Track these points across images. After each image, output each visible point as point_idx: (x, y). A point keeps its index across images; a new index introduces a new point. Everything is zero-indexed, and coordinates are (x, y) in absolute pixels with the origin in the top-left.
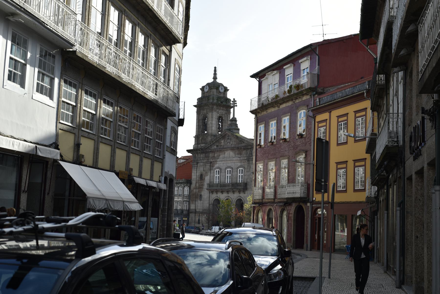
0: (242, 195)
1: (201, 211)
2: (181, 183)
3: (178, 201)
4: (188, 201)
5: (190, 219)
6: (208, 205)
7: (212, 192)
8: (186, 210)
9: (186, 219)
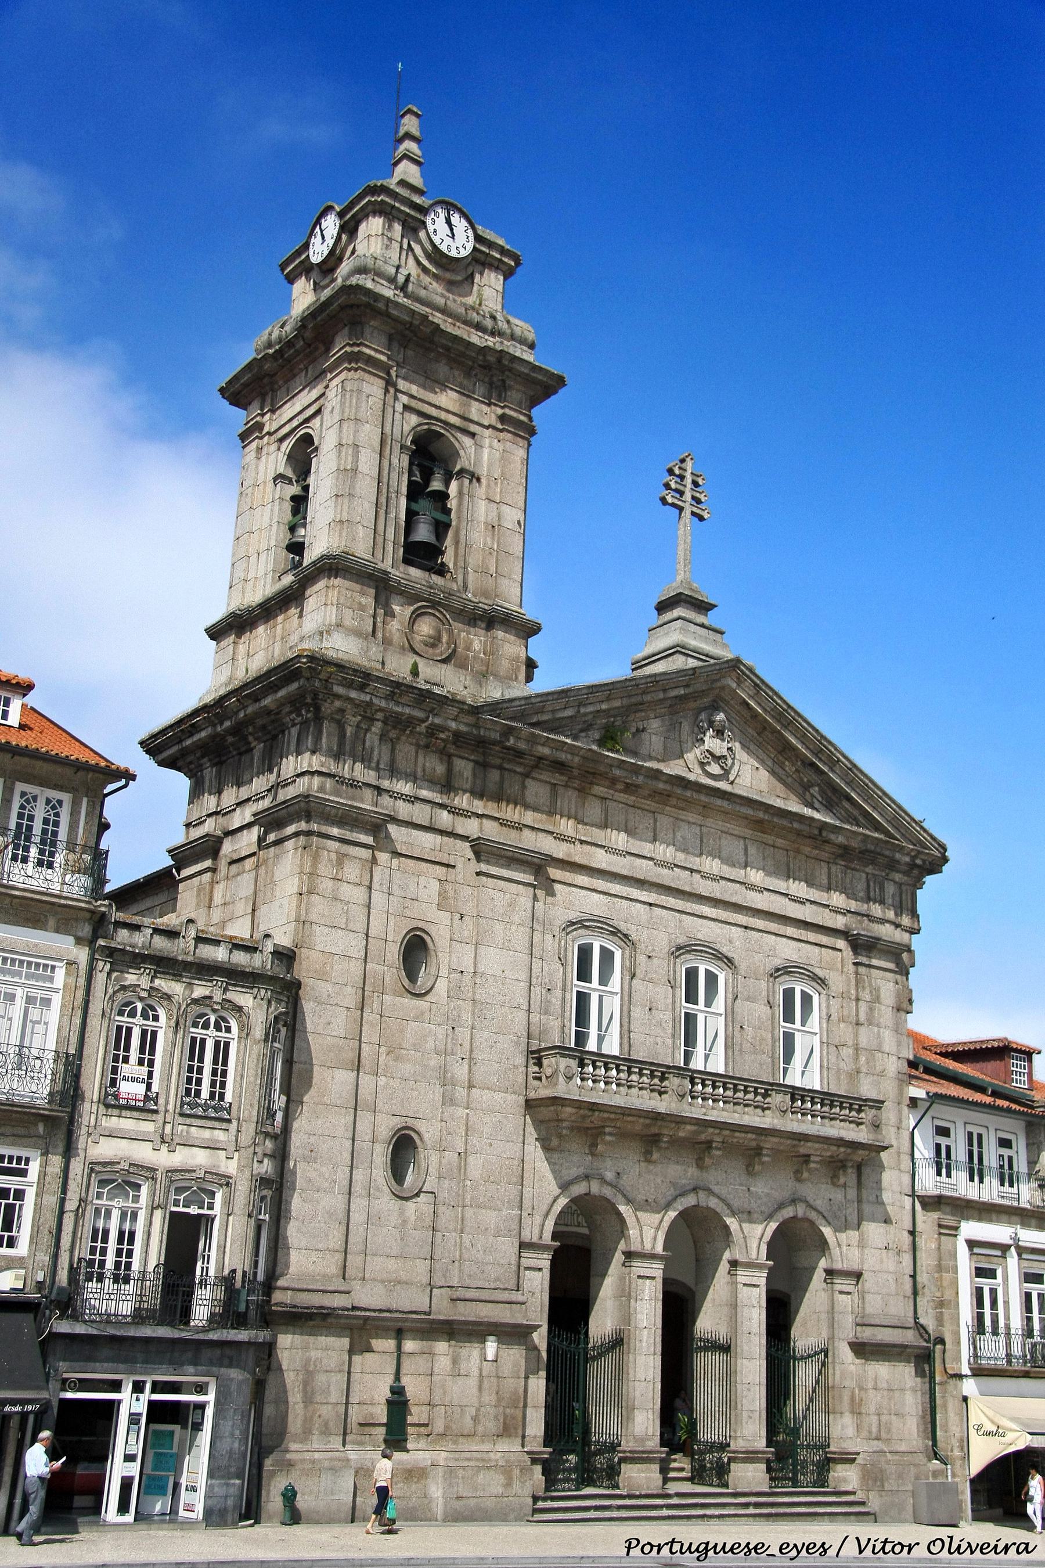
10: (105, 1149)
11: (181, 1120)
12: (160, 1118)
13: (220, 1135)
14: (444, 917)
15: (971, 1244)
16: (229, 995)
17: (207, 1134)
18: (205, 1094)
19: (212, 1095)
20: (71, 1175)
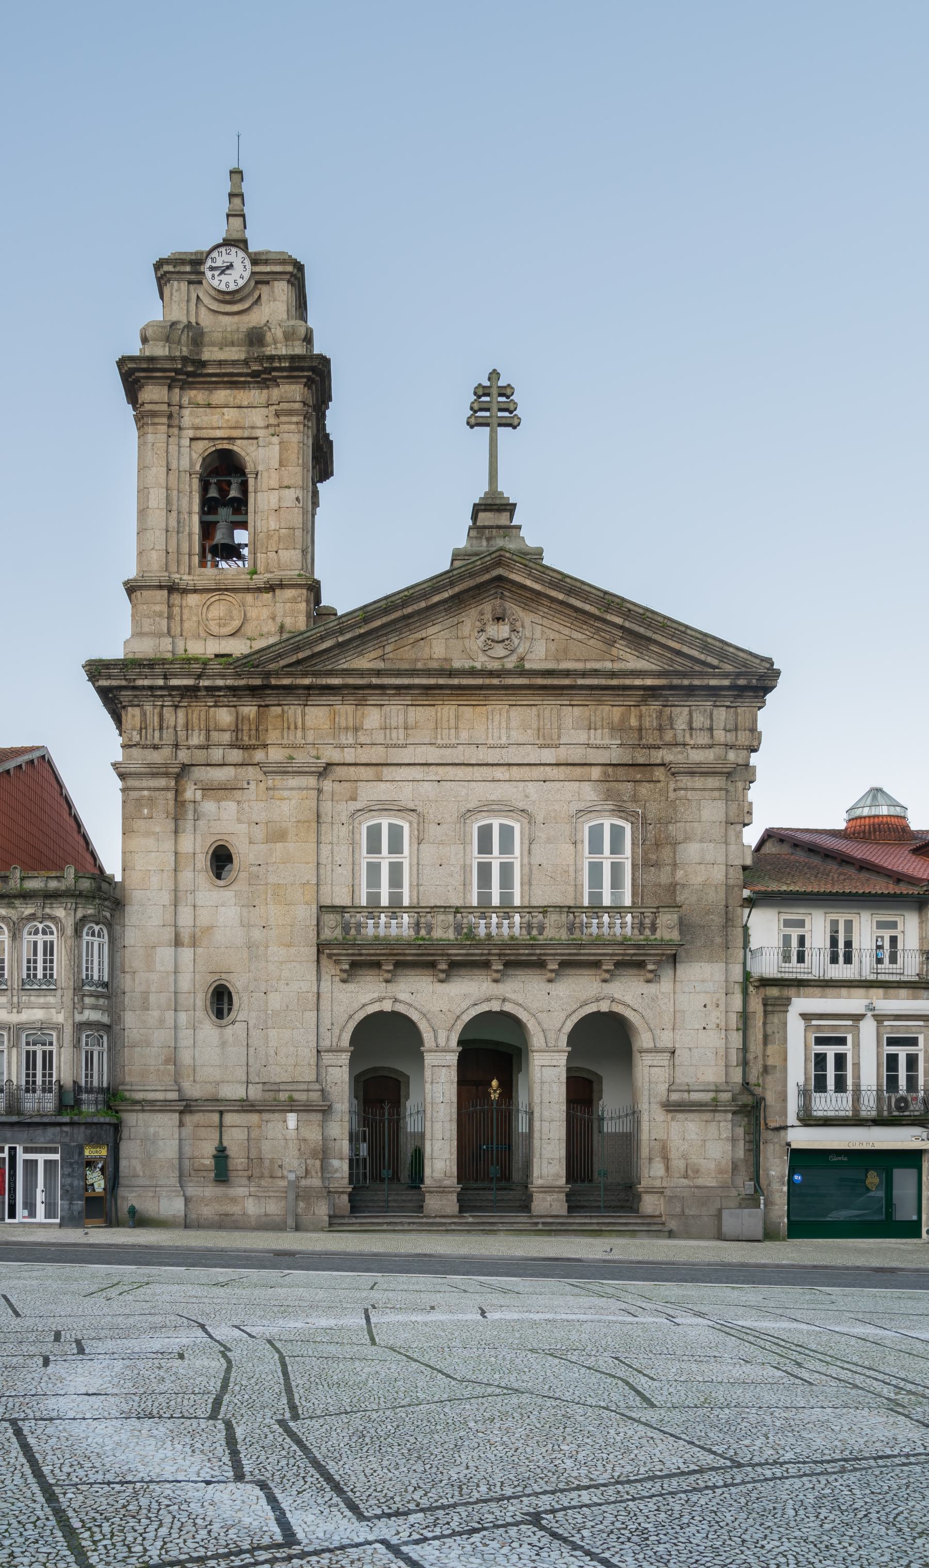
0: (627, 995)
1: (234, 1091)
3: (20, 1028)
4: (108, 1028)
5: (130, 1150)
6: (309, 1054)
9: (104, 1152)
11: (23, 993)
12: (9, 992)
13: (51, 999)
14: (243, 828)
15: (806, 1017)
16: (47, 910)
17: (42, 1000)
18: (40, 975)
19: (45, 976)
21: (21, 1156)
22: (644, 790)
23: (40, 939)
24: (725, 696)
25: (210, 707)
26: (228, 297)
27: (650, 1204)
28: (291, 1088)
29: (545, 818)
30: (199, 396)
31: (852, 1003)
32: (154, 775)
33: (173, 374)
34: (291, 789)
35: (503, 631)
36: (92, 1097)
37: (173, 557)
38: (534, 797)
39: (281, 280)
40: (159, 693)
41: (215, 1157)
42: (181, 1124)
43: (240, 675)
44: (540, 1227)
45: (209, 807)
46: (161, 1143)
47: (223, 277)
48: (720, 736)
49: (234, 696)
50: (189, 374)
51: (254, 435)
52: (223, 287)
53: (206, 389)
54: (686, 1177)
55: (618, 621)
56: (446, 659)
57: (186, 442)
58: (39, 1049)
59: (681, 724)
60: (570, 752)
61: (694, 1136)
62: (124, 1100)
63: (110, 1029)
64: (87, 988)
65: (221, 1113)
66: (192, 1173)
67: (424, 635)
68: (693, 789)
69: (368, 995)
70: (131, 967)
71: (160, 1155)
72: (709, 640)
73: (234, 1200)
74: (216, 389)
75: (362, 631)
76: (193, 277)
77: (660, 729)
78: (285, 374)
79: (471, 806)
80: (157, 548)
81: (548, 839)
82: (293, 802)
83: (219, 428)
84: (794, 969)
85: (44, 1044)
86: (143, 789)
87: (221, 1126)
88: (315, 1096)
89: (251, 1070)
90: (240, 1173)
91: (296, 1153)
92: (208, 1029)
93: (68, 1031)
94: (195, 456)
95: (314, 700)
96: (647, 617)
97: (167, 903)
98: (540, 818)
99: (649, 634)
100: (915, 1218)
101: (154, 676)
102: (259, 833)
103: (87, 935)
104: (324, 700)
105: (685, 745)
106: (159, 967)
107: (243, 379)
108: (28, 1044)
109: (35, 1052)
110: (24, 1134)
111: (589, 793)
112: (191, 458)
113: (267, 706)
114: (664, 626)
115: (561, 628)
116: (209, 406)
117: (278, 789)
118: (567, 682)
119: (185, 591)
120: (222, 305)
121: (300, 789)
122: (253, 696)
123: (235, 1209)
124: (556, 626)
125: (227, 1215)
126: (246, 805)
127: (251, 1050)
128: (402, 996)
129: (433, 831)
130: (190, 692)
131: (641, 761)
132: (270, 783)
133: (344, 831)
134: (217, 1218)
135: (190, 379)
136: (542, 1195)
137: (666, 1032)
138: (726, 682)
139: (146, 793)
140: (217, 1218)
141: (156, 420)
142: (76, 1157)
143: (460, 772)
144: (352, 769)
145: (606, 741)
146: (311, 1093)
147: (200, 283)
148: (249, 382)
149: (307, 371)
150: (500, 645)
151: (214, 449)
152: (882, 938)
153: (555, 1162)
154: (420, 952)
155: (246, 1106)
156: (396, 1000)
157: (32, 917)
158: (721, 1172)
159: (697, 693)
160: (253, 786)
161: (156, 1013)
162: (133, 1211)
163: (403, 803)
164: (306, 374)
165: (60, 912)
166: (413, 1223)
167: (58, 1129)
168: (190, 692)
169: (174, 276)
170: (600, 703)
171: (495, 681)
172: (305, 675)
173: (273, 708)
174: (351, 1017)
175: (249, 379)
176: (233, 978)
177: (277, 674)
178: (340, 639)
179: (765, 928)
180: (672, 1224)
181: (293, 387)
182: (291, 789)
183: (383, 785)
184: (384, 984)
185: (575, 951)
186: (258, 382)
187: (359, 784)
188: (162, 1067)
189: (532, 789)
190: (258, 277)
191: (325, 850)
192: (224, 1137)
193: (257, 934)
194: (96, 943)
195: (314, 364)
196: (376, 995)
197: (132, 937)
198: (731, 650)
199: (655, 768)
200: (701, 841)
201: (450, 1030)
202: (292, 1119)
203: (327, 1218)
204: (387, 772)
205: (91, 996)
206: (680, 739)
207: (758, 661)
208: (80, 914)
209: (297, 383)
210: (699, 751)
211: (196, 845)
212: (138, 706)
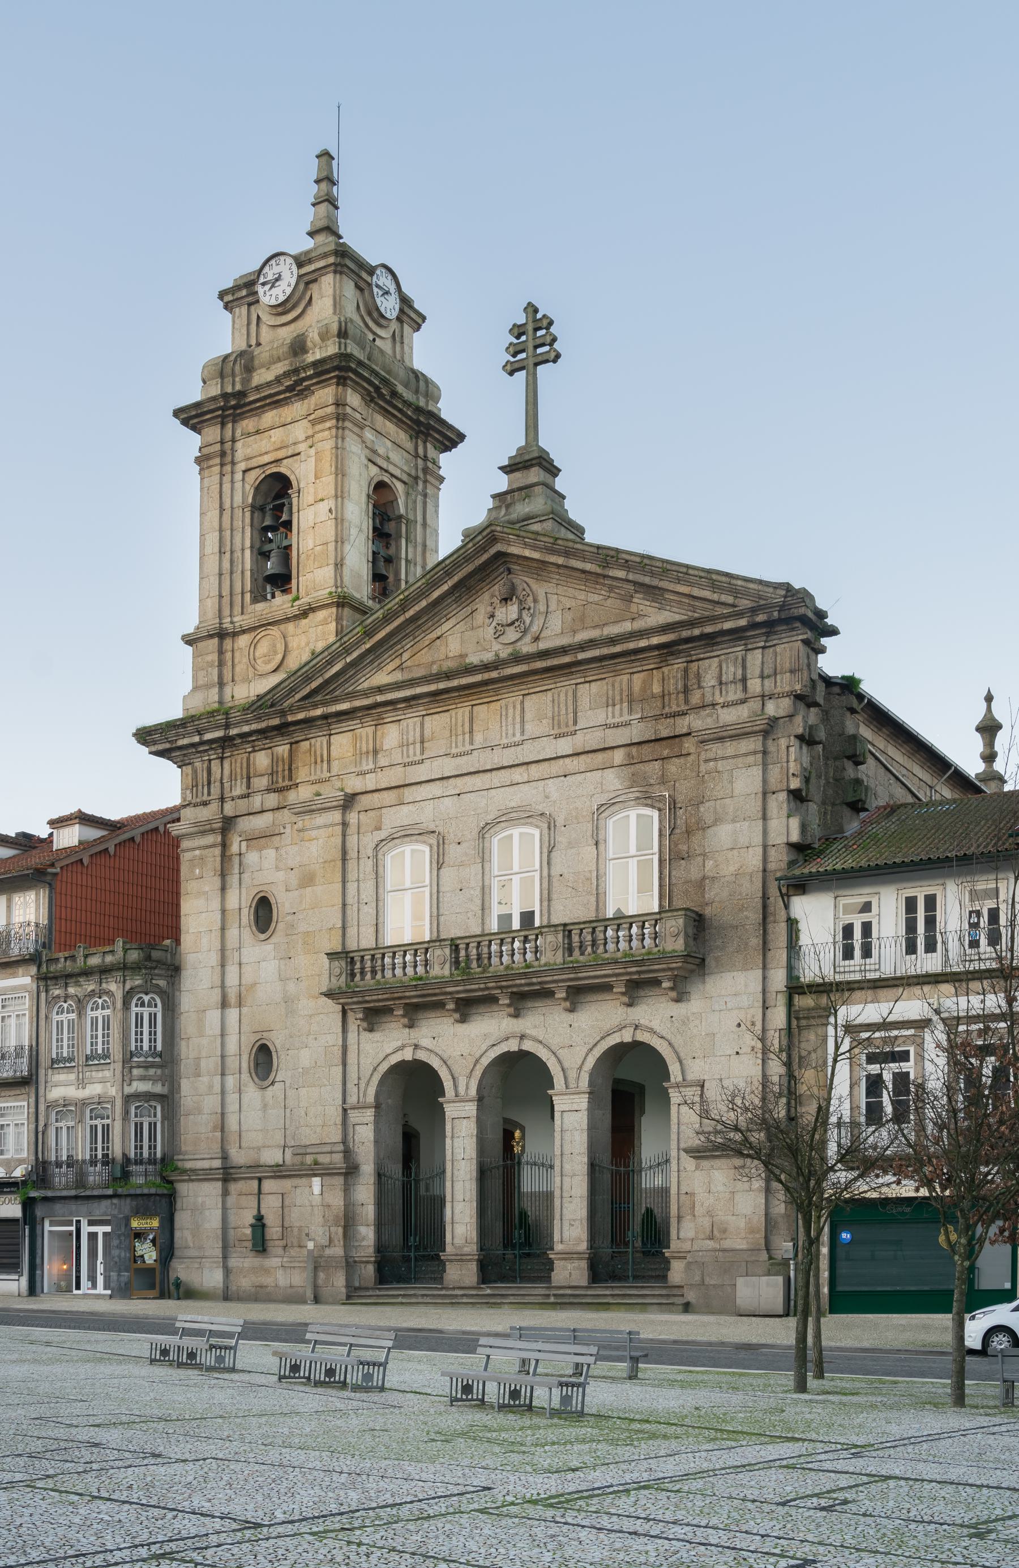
0: (655, 1019)
1: (272, 1157)
2: (104, 971)
3: (83, 1103)
5: (182, 1219)
6: (335, 1114)
7: (374, 1016)
8: (152, 1161)
9: (155, 1223)
10: (55, 1093)
17: (100, 1074)
20: (40, 1111)
21: (86, 1229)
22: (673, 767)
23: (99, 1013)
24: (753, 637)
25: (249, 753)
26: (280, 309)
27: (677, 1272)
28: (316, 1150)
29: (566, 819)
30: (248, 424)
31: (911, 1007)
32: (203, 833)
33: (220, 412)
34: (319, 828)
35: (512, 611)
36: (141, 1168)
37: (226, 600)
38: (555, 796)
39: (327, 273)
40: (201, 749)
41: (252, 1226)
42: (225, 1193)
43: (260, 718)
44: (552, 1300)
45: (252, 858)
46: (207, 1213)
47: (274, 291)
48: (755, 685)
49: (266, 738)
50: (235, 407)
51: (297, 452)
52: (273, 302)
53: (255, 415)
54: (711, 1238)
55: (621, 574)
56: (461, 656)
57: (239, 476)
58: (98, 1122)
59: (709, 680)
60: (588, 736)
61: (721, 1188)
62: (176, 1169)
63: (168, 1101)
64: (136, 1059)
65: (260, 1180)
66: (237, 1243)
67: (439, 634)
68: (723, 758)
69: (388, 1045)
70: (186, 1033)
71: (207, 1226)
72: (714, 577)
73: (267, 1271)
74: (264, 412)
75: (368, 646)
76: (251, 299)
77: (686, 691)
78: (314, 381)
79: (489, 818)
80: (211, 595)
81: (570, 843)
82: (321, 841)
83: (266, 453)
84: (854, 969)
85: (103, 1118)
86: (194, 849)
87: (260, 1192)
88: (338, 1158)
89: (288, 1132)
90: (277, 1243)
91: (321, 1219)
92: (252, 1093)
93: (119, 1103)
94: (247, 487)
95: (336, 728)
96: (645, 563)
97: (214, 964)
98: (560, 821)
99: (655, 582)
100: (1008, 1286)
101: (190, 735)
102: (294, 879)
103: (136, 1006)
104: (344, 726)
105: (713, 705)
106: (208, 1032)
107: (282, 396)
108: (91, 1118)
109: (96, 1126)
110: (84, 1207)
111: (613, 781)
112: (243, 491)
113: (297, 742)
114: (666, 571)
115: (577, 593)
116: (258, 432)
117: (307, 830)
118: (567, 659)
119: (235, 634)
120: (278, 318)
121: (325, 826)
122: (282, 735)
123: (268, 1281)
124: (571, 592)
125: (261, 1287)
126: (283, 851)
127: (288, 1111)
128: (425, 1042)
129: (453, 852)
130: (226, 743)
131: (665, 733)
132: (300, 825)
133: (368, 865)
134: (253, 1289)
135: (238, 411)
136: (562, 1263)
137: (697, 1061)
138: (743, 622)
139: (197, 852)
140: (253, 1289)
141: (211, 463)
142: (123, 1229)
143: (477, 781)
144: (376, 795)
145: (626, 718)
146: (334, 1155)
147: (258, 301)
148: (289, 398)
149: (334, 371)
150: (512, 628)
151: (263, 476)
152: (978, 913)
153: (577, 1223)
154: (419, 993)
155: (279, 1172)
156: (416, 1047)
157: (92, 994)
158: (752, 1231)
159: (718, 640)
160: (288, 830)
161: (205, 1079)
162: (178, 1284)
163: (424, 826)
164: (333, 374)
165: (113, 987)
166: (427, 1295)
167: (109, 1201)
168: (226, 743)
169: (235, 303)
170: (617, 673)
171: (494, 674)
172: (315, 706)
173: (302, 743)
174: (477, 1061)
175: (288, 395)
176: (273, 1036)
177: (291, 710)
178: (348, 660)
179: (818, 917)
180: (691, 1296)
181: (326, 390)
182: (319, 828)
183: (405, 809)
184: (407, 1030)
185: (572, 976)
186: (297, 395)
187: (384, 810)
188: (211, 1135)
189: (552, 786)
190: (306, 278)
191: (352, 887)
192: (262, 1205)
193: (291, 987)
194: (149, 1009)
195: (335, 364)
196: (399, 1043)
197: (187, 1002)
198: (740, 583)
199: (684, 739)
200: (734, 821)
201: (470, 1076)
202: (316, 1182)
203: (344, 1290)
204: (409, 794)
205: (139, 1067)
206: (709, 699)
207: (771, 590)
208: (128, 987)
209: (329, 385)
210: (731, 709)
211: (240, 900)
212: (189, 764)
